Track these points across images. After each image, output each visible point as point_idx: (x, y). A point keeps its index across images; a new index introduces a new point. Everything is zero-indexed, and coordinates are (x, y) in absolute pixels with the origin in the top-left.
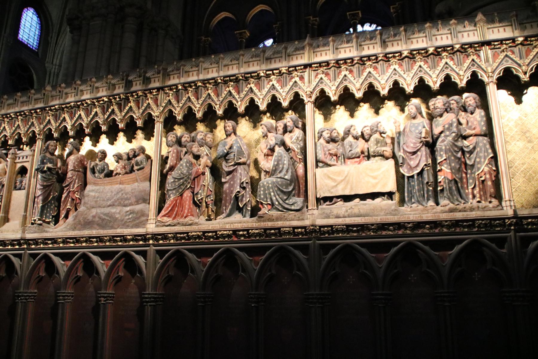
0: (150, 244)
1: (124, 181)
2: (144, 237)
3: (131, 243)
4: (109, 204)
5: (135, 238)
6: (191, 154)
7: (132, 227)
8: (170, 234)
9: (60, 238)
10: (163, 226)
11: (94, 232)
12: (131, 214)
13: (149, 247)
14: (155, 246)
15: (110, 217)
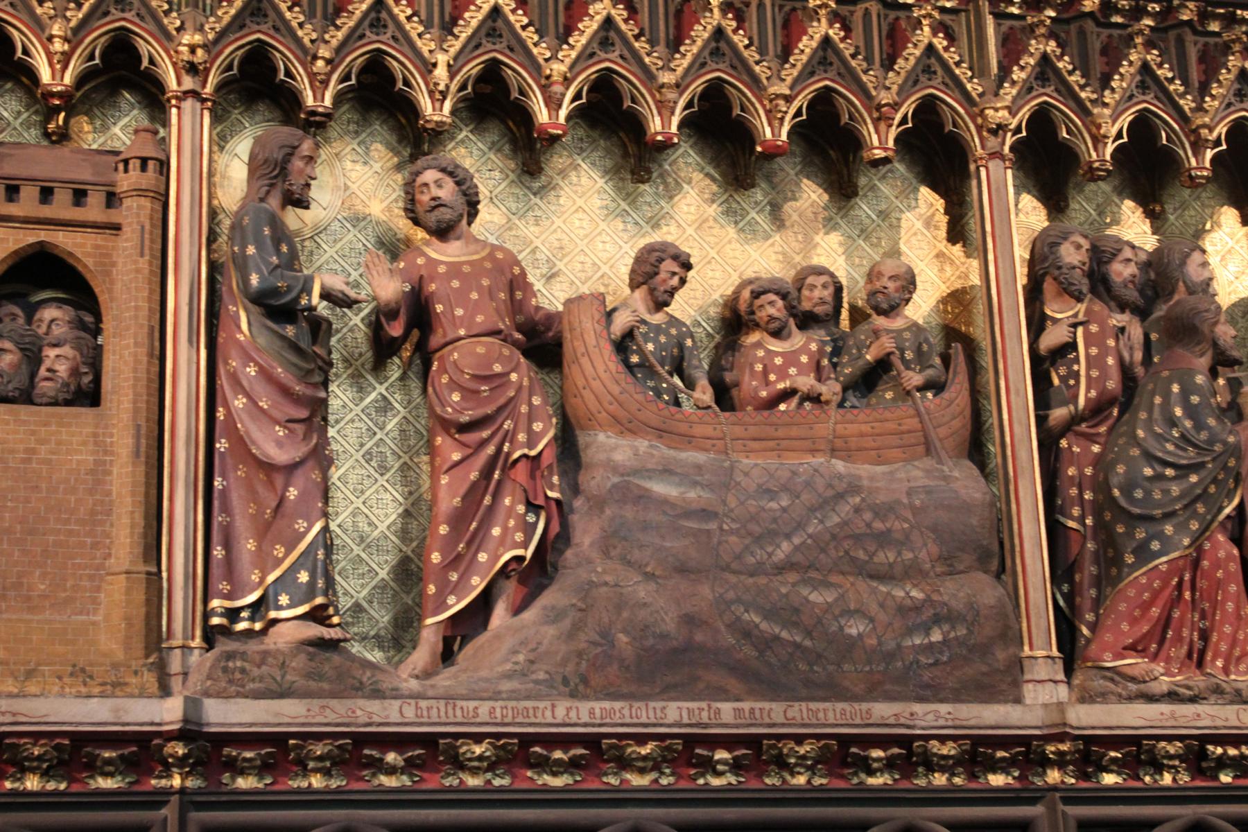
0: (1054, 788)
1: (853, 442)
2: (1027, 752)
3: (940, 780)
4: (780, 555)
5: (978, 752)
6: (1209, 354)
7: (957, 696)
8: (1170, 739)
9: (478, 738)
10: (1130, 699)
11: (727, 714)
12: (937, 620)
13: (1032, 801)
14: (1067, 801)
15: (808, 633)
